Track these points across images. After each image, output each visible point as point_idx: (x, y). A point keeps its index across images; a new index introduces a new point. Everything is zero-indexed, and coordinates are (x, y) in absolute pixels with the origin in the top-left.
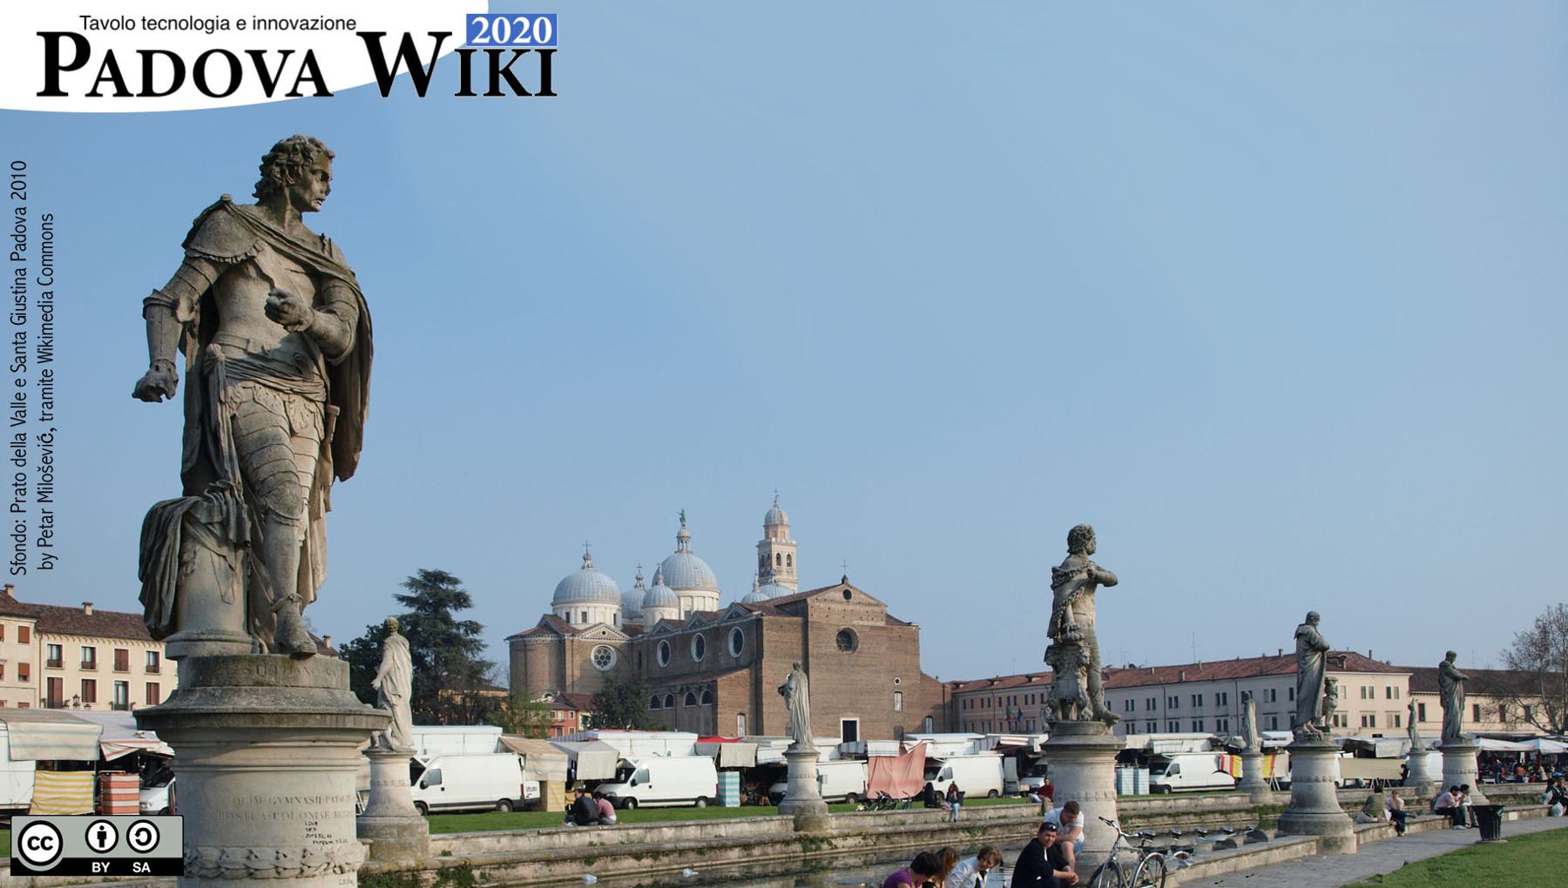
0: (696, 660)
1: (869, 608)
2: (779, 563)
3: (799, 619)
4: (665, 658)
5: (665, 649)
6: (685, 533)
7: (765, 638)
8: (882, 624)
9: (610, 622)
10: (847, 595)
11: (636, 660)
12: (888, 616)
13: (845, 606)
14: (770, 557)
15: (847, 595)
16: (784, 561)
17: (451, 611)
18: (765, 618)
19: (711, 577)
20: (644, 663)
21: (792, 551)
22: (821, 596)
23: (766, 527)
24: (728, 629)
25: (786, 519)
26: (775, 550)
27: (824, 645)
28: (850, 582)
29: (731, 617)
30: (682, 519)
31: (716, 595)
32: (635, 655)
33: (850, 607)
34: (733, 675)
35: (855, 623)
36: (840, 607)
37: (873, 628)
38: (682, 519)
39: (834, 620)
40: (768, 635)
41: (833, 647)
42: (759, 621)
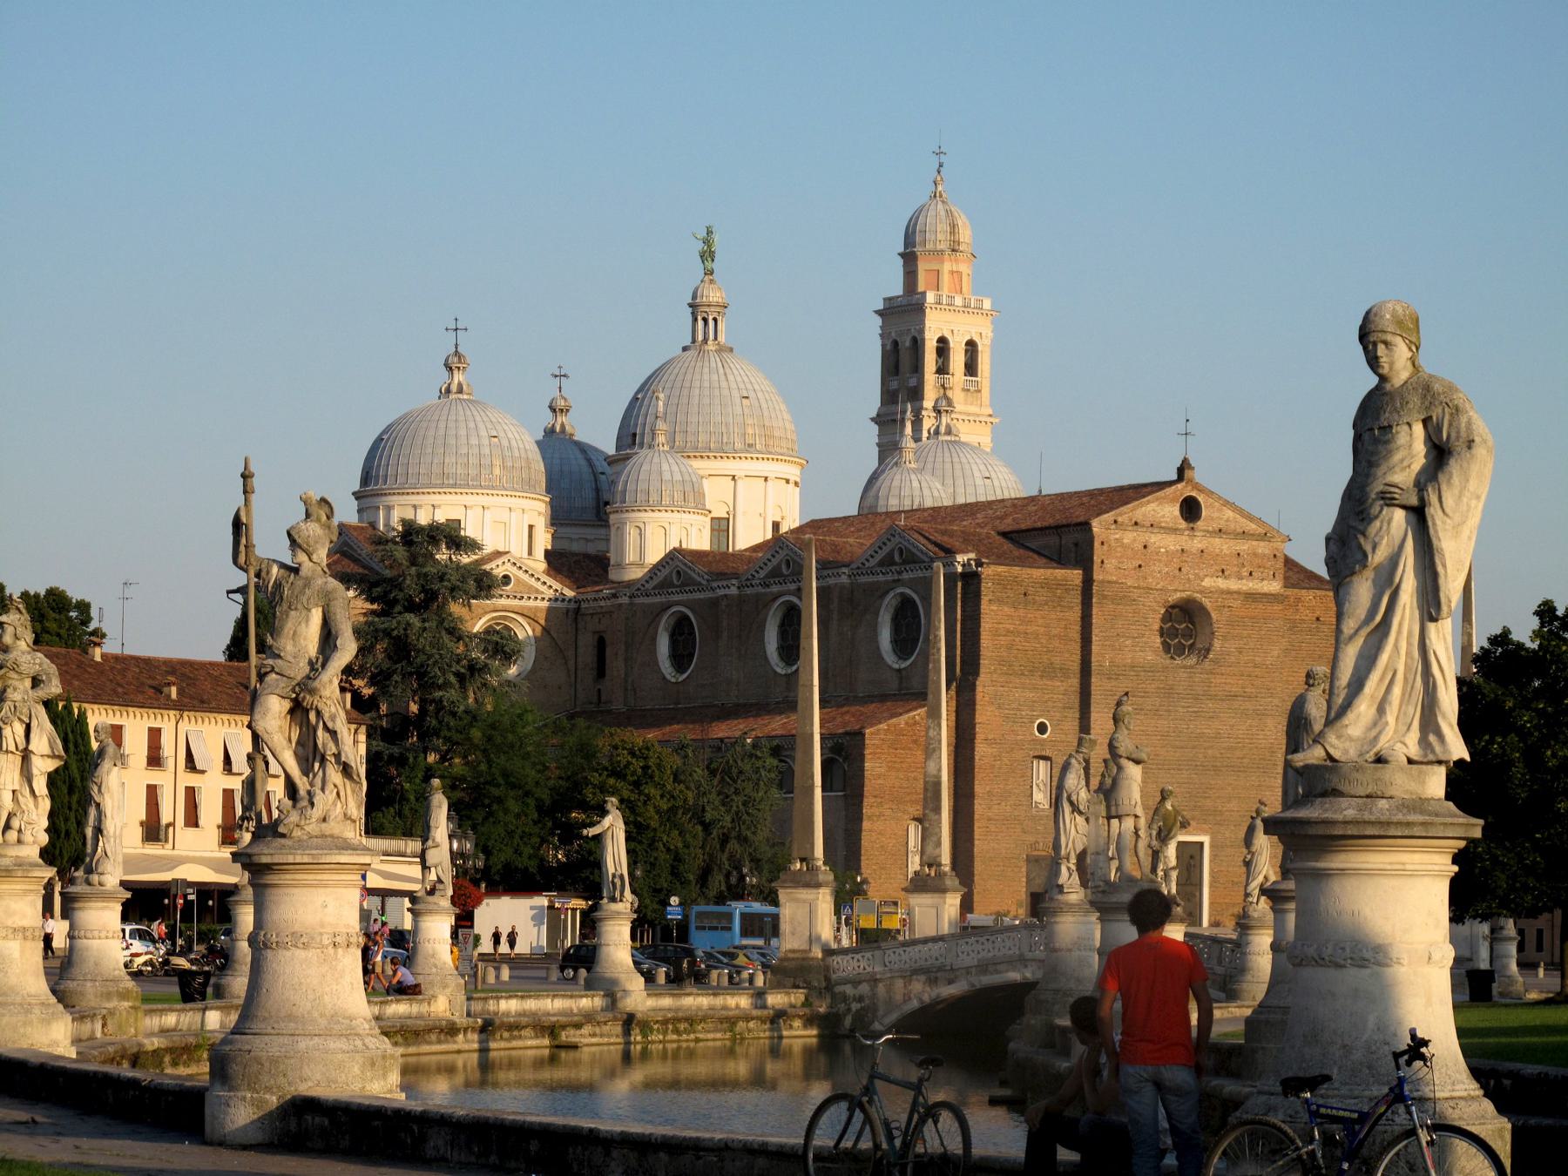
0: (780, 669)
1: (1244, 546)
2: (942, 370)
3: (1075, 575)
4: (680, 658)
5: (681, 630)
6: (713, 295)
7: (986, 625)
8: (1275, 587)
9: (518, 548)
10: (1190, 509)
11: (587, 655)
12: (1289, 563)
13: (1183, 541)
14: (917, 345)
15: (1190, 509)
16: (957, 360)
17: (455, 608)
18: (987, 572)
19: (782, 419)
20: (616, 665)
21: (979, 328)
22: (1126, 513)
23: (909, 259)
24: (880, 591)
25: (965, 235)
26: (935, 325)
27: (1130, 642)
28: (1198, 474)
29: (888, 561)
30: (707, 255)
31: (793, 472)
32: (587, 642)
33: (1197, 544)
34: (902, 721)
35: (1209, 585)
36: (1169, 543)
37: (1251, 597)
38: (707, 255)
39: (1157, 575)
40: (991, 614)
41: (1149, 648)
42: (971, 579)
